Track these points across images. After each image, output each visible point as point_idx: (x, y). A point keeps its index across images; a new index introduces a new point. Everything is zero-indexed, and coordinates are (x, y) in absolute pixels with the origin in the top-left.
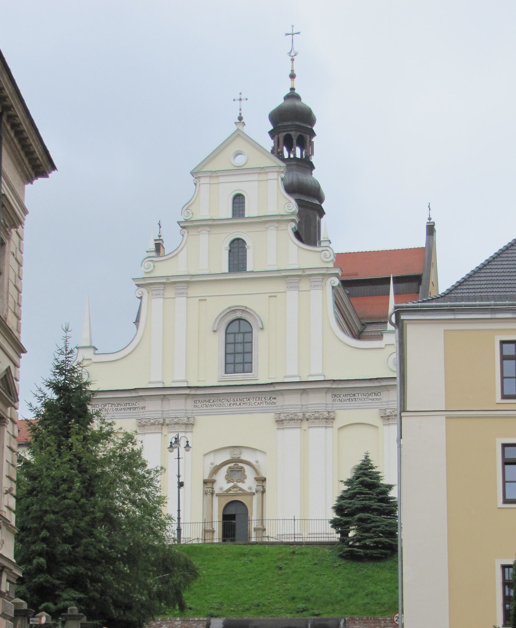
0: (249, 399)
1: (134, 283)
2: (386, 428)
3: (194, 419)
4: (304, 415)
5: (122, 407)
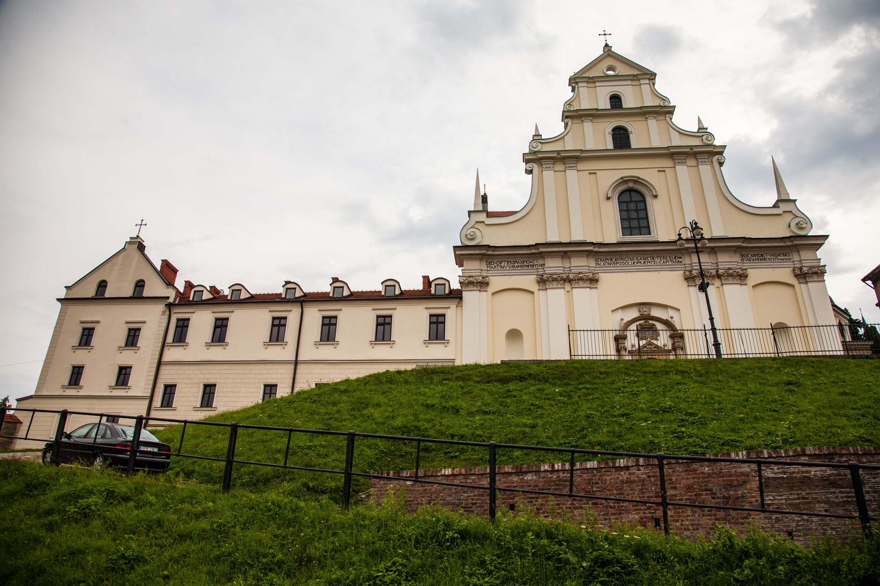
0: (653, 258)
5: (519, 264)
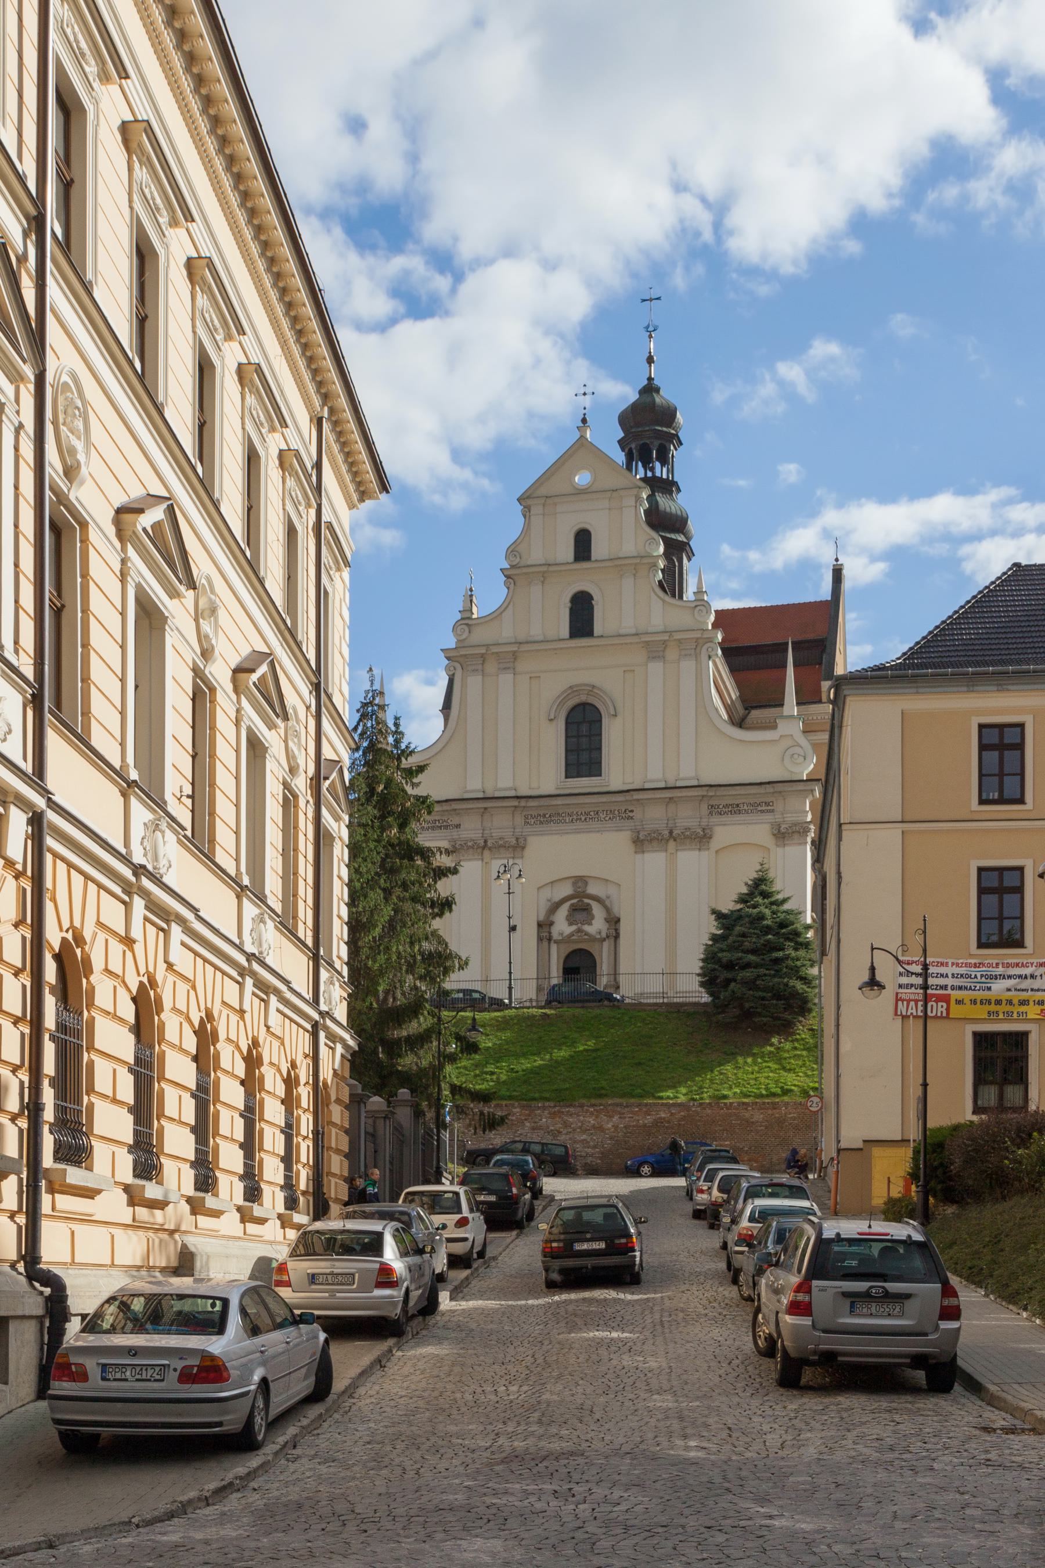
1: (442, 654)
2: (780, 850)
3: (525, 840)
4: (671, 832)
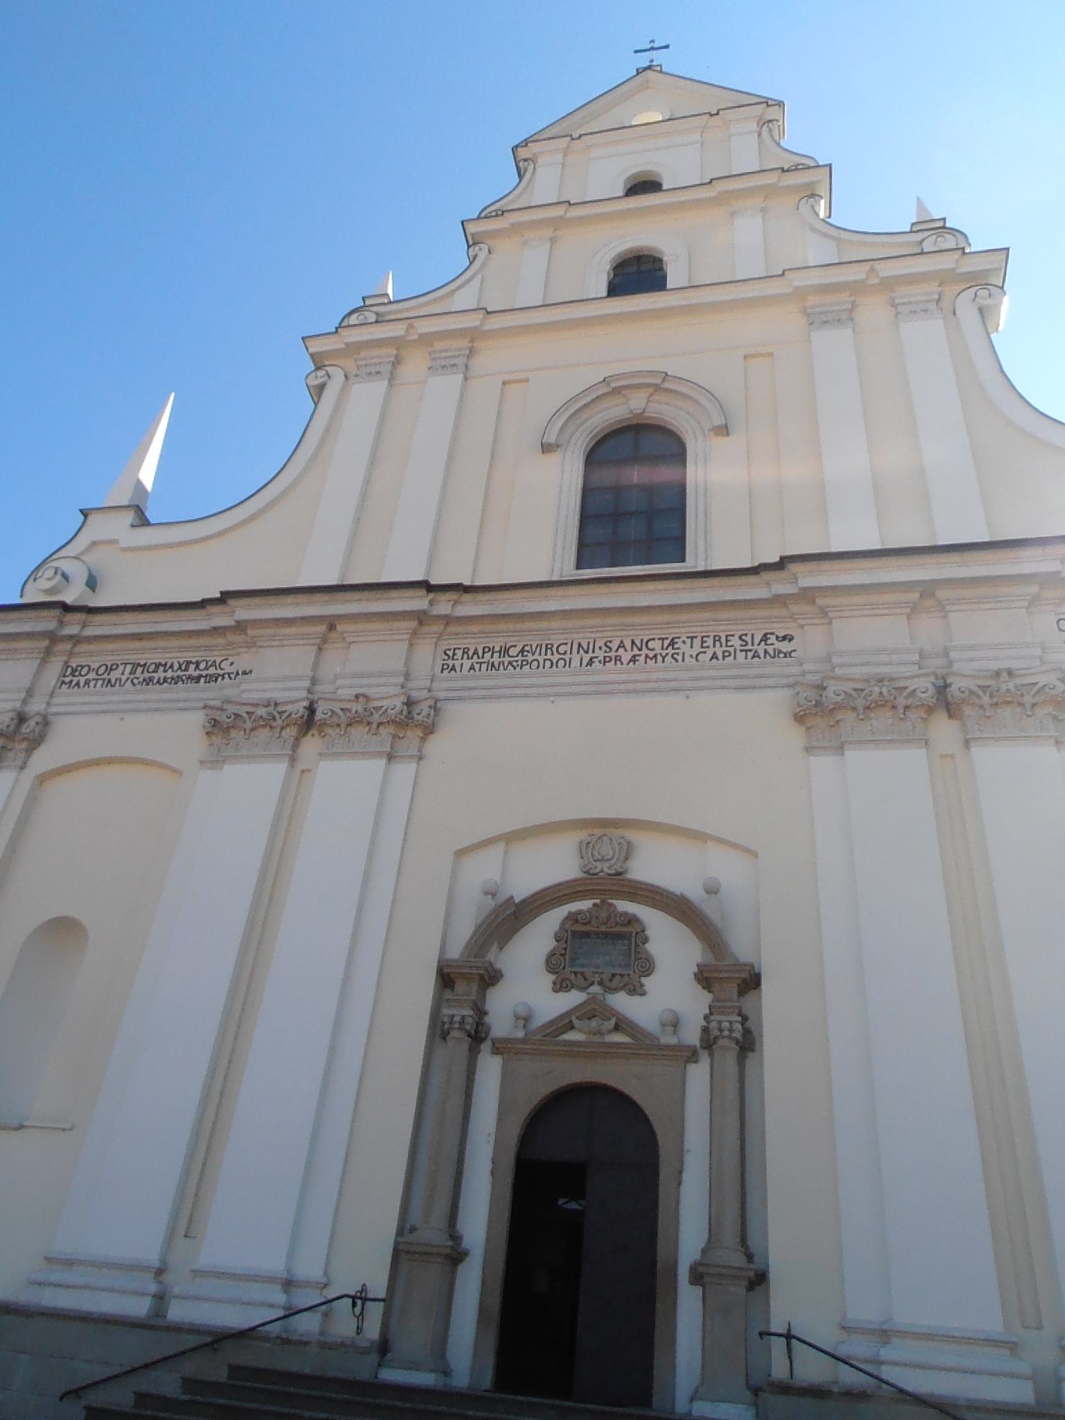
0: (672, 643)
3: (435, 709)
